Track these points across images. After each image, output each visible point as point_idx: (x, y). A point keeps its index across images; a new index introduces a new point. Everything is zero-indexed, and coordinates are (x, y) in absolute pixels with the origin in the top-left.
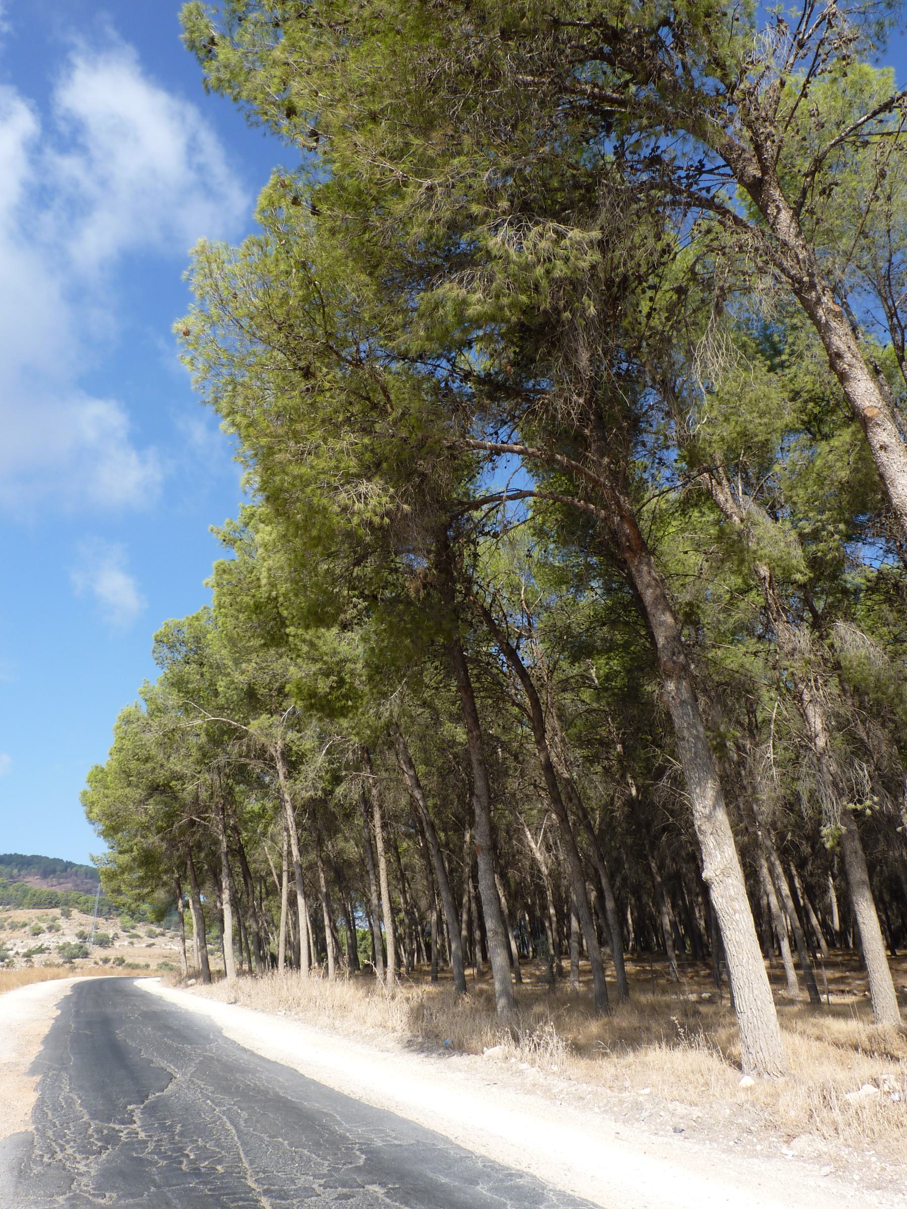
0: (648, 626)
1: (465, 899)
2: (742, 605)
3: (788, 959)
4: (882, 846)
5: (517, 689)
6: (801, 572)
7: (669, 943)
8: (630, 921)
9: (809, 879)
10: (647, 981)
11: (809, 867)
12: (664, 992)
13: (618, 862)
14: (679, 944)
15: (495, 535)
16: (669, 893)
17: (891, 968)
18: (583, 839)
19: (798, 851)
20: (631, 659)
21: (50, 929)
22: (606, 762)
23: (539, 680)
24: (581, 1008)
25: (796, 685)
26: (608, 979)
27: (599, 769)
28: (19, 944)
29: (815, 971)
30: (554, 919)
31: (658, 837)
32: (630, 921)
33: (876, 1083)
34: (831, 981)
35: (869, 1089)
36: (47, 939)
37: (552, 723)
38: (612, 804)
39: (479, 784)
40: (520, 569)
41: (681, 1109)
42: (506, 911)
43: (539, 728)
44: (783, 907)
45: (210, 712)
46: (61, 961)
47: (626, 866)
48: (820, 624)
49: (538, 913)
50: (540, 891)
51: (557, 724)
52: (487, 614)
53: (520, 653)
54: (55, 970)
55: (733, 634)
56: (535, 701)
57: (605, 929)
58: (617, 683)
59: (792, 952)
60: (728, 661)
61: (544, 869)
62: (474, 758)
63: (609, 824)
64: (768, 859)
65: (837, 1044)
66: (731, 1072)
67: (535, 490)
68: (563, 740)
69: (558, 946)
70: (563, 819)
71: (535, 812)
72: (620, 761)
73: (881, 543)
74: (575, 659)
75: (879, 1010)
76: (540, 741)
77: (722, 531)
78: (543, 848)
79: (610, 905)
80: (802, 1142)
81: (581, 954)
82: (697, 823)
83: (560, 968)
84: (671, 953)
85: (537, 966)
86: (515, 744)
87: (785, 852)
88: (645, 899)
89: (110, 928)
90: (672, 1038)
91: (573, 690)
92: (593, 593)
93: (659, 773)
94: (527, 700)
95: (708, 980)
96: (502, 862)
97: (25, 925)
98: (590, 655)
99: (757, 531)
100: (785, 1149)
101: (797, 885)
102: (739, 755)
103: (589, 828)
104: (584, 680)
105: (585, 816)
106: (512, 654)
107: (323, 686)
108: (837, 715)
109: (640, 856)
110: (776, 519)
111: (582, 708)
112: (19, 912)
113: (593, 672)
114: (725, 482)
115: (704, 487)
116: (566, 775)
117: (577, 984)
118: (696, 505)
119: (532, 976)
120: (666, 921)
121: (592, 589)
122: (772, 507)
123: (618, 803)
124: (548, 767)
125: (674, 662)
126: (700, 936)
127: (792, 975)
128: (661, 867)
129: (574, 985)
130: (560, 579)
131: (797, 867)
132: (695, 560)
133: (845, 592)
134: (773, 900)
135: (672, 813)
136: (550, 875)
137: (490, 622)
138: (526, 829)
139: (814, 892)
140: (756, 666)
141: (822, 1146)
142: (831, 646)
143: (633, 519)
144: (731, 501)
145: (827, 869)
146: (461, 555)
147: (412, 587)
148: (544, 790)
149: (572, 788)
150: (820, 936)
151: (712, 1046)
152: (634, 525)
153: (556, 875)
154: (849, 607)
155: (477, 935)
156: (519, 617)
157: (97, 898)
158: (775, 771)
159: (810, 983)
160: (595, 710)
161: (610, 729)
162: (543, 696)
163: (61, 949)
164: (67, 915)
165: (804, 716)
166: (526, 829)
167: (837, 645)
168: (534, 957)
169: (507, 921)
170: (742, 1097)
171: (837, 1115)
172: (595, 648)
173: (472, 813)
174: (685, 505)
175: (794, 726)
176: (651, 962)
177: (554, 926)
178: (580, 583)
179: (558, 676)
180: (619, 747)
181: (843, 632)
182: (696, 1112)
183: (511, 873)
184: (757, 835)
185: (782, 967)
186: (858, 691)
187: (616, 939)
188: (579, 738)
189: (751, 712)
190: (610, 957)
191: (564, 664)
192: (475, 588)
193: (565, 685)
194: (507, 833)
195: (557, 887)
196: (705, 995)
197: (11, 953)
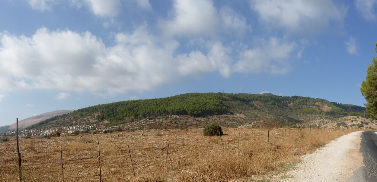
21: (355, 120)
28: (349, 123)
36: (355, 123)
46: (358, 127)
54: (357, 129)
89: (368, 121)
97: (350, 120)
112: (348, 117)
157: (364, 114)
163: (358, 125)
164: (358, 117)
197: (348, 125)
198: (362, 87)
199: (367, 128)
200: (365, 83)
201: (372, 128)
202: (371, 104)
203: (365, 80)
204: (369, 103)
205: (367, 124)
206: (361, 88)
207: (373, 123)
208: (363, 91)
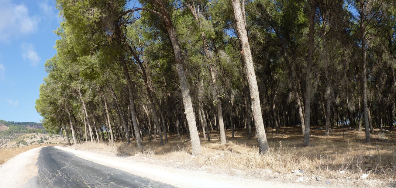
0: (173, 50)
1: (129, 122)
2: (198, 45)
3: (204, 132)
4: (226, 107)
5: (139, 69)
6: (213, 35)
7: (178, 130)
8: (168, 126)
9: (210, 115)
10: (172, 138)
11: (210, 112)
12: (176, 140)
13: (165, 112)
14: (180, 130)
15: (131, 23)
16: (178, 119)
17: (225, 133)
18: (157, 107)
19: (208, 108)
20: (169, 60)
22: (162, 87)
23: (145, 66)
24: (157, 145)
25: (209, 66)
26: (163, 139)
27: (161, 89)
29: (210, 134)
30: (150, 126)
31: (175, 105)
32: (168, 126)
33: (219, 154)
34: (213, 136)
35: (218, 156)
37: (149, 77)
38: (164, 97)
39: (131, 94)
40: (138, 34)
41: (178, 163)
42: (139, 125)
43: (145, 79)
44: (204, 121)
45: (61, 82)
47: (167, 113)
48: (216, 51)
49: (147, 125)
50: (147, 120)
51: (150, 77)
52: (130, 47)
53: (140, 59)
55: (196, 53)
56: (144, 72)
57: (162, 128)
58: (165, 66)
59: (205, 131)
60: (194, 60)
61: (148, 114)
62: (129, 87)
63: (163, 102)
64: (201, 110)
65: (213, 148)
66: (190, 155)
67: (141, 7)
68: (151, 82)
69: (151, 132)
70: (152, 101)
71: (145, 100)
72: (166, 87)
73: (233, 30)
74: (154, 60)
75: (222, 141)
76: (146, 82)
77: (193, 22)
78: (147, 110)
79: (163, 121)
80: (203, 167)
81: (157, 134)
82: (184, 100)
83: (152, 137)
84: (178, 132)
85: (147, 137)
86: (139, 83)
87: (205, 108)
88: (173, 120)
90: (177, 149)
91: (154, 68)
92: (159, 40)
93: (176, 89)
94: (142, 71)
95: (186, 137)
96: (137, 114)
98: (158, 59)
99: (202, 23)
100: (200, 169)
101: (207, 116)
102: (195, 85)
103: (158, 104)
104: (157, 65)
105: (157, 101)
106: (137, 59)
107: (89, 72)
108: (218, 75)
109: (171, 110)
110: (208, 20)
111: (156, 73)
113: (159, 63)
114: (194, 7)
115: (189, 8)
116: (152, 91)
117: (156, 140)
118: (187, 14)
119: (145, 139)
120: (177, 125)
121: (158, 39)
122: (207, 16)
123: (165, 98)
124: (148, 89)
125: (179, 59)
126: (185, 128)
127: (205, 135)
128: (176, 113)
129: (156, 140)
130: (150, 36)
131: (207, 112)
132: (185, 30)
133: (223, 42)
134: (201, 119)
135: (178, 99)
136: (149, 116)
137: (131, 50)
138: (143, 105)
139: (211, 117)
140: (200, 62)
141: (207, 167)
142: (218, 57)
143: (169, 17)
144: (196, 13)
145: (214, 112)
146: (122, 30)
147: (109, 40)
148: (147, 94)
149: (154, 94)
150: (212, 127)
151: (186, 150)
152: (169, 19)
153: (150, 116)
154: (223, 47)
155: (132, 131)
156: (139, 48)
158: (203, 88)
159: (209, 137)
160: (159, 74)
161: (163, 79)
162: (146, 70)
165: (211, 75)
166: (143, 105)
167: (220, 56)
168: (146, 135)
169: (139, 127)
170: (191, 160)
171: (211, 161)
172: (159, 57)
173: (129, 102)
174: (184, 14)
175: (209, 78)
176: (174, 134)
177: (150, 127)
178: (155, 37)
179: (150, 65)
180: (166, 84)
181: (221, 53)
182: (181, 163)
183: (140, 116)
184: (199, 104)
185: (203, 134)
186: (224, 70)
187: (165, 130)
188: (155, 81)
189: (199, 74)
190: (164, 134)
191: (151, 61)
192: (127, 40)
193: (152, 68)
194: (138, 106)
195: (151, 119)
196: (185, 141)
198: (36, 105)
199: (47, 143)
200: (38, 100)
201: (52, 143)
202: (48, 120)
203: (38, 97)
204: (45, 119)
205: (46, 139)
206: (36, 106)
207: (53, 137)
208: (38, 108)
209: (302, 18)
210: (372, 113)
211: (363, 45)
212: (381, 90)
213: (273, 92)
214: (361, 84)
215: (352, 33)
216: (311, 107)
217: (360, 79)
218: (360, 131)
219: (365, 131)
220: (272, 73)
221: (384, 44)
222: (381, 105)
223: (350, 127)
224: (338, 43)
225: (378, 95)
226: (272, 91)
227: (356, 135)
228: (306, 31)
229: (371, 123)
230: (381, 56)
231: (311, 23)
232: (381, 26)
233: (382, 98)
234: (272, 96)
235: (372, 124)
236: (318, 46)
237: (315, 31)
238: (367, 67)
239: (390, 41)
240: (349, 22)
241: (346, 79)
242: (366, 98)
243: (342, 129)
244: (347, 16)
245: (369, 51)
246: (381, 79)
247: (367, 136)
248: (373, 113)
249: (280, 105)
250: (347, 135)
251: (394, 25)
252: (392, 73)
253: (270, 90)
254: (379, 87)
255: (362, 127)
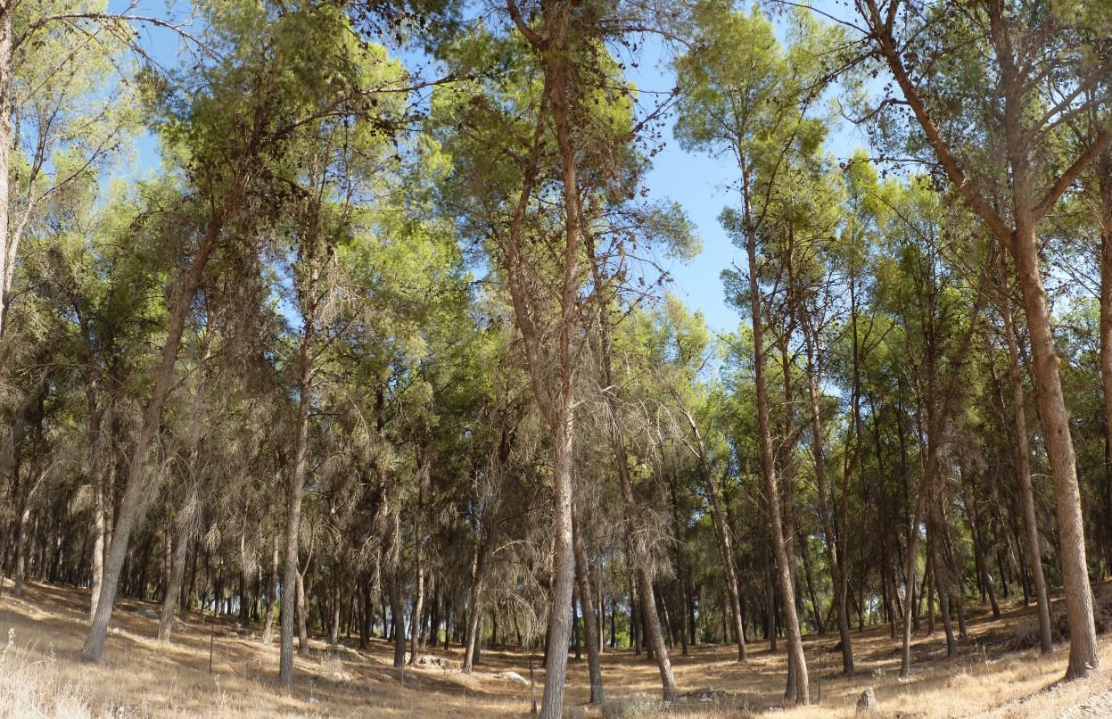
209: (155, 307)
210: (313, 589)
211: (304, 401)
212: (342, 523)
213: (33, 474)
214: (287, 501)
215: (279, 366)
216: (129, 546)
217: (287, 485)
218: (266, 642)
219: (280, 642)
220: (44, 422)
221: (359, 402)
222: (339, 568)
223: (239, 625)
224: (239, 385)
225: (331, 539)
226: (32, 469)
227: (251, 655)
228: (159, 339)
229: (302, 623)
230: (350, 432)
231: (176, 326)
232: (357, 359)
233: (345, 549)
234: (29, 483)
235: (308, 625)
236: (182, 383)
237: (182, 347)
238: (307, 456)
239: (380, 397)
240: (274, 338)
241: (243, 479)
242: (295, 543)
243: (209, 628)
244: (273, 325)
245: (320, 417)
246: (345, 493)
247: (285, 660)
248: (316, 590)
249: (46, 513)
250: (224, 648)
251: (392, 359)
252: (380, 477)
253: (28, 465)
254: (338, 513)
255: (274, 631)
